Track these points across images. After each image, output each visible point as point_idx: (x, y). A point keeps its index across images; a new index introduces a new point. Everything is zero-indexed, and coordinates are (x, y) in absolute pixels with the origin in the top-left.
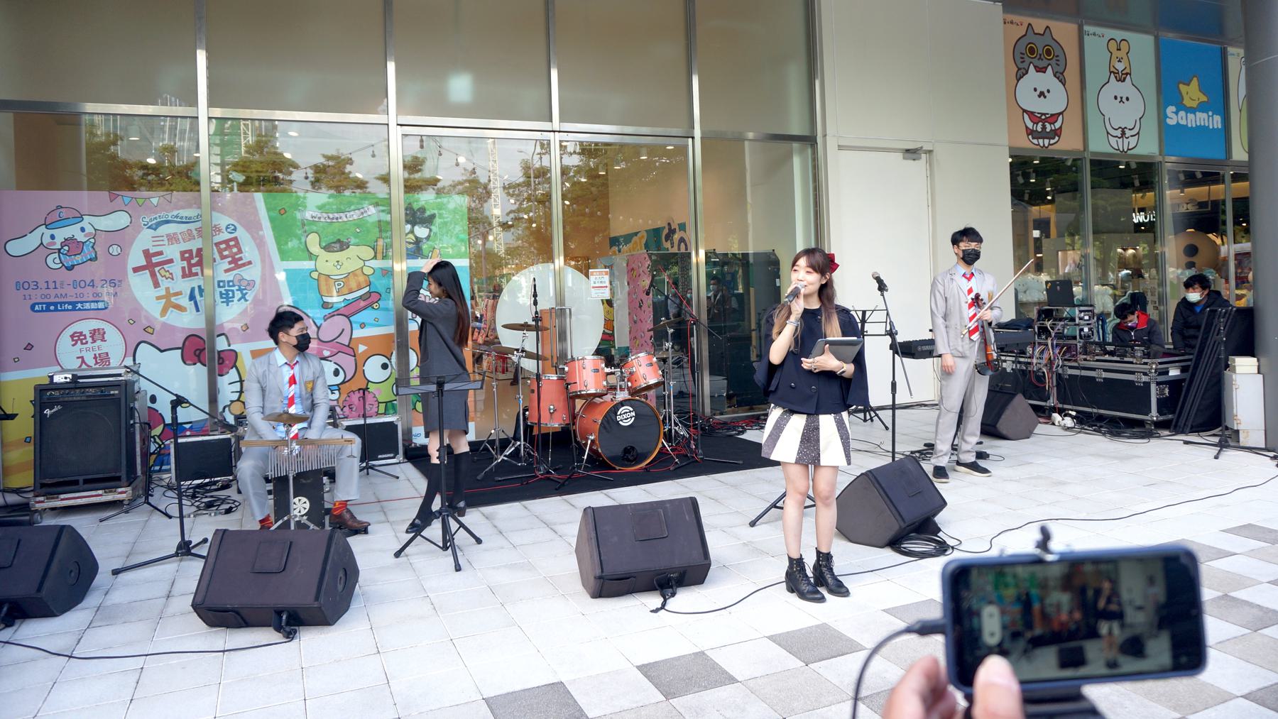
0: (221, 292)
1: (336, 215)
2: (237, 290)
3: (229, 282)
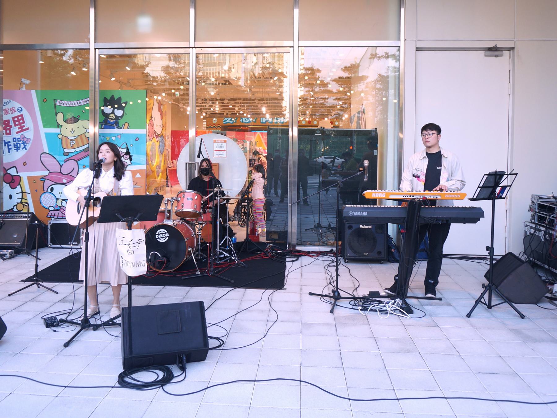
0: (14, 144)
1: (72, 102)
2: (22, 143)
3: (18, 138)
